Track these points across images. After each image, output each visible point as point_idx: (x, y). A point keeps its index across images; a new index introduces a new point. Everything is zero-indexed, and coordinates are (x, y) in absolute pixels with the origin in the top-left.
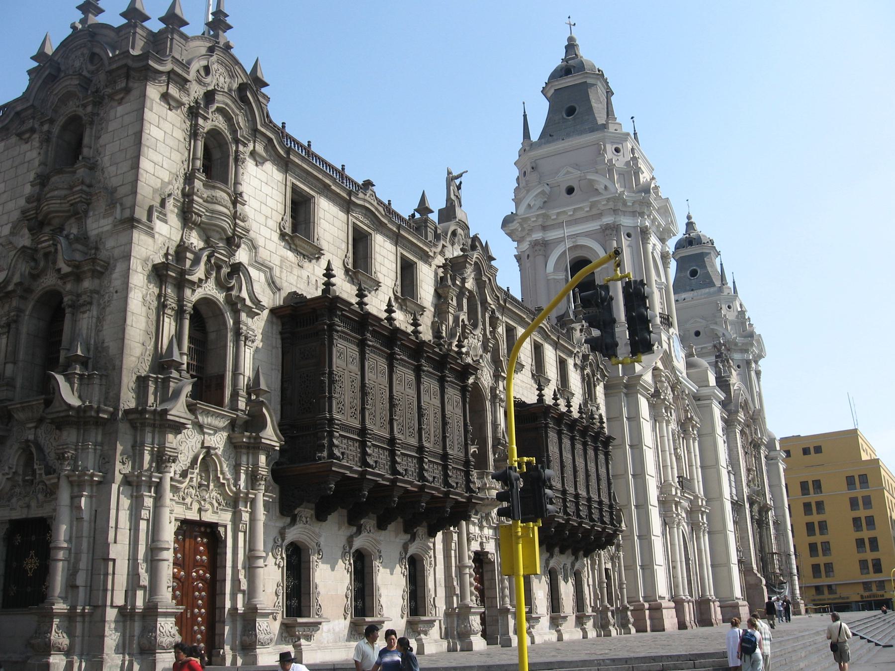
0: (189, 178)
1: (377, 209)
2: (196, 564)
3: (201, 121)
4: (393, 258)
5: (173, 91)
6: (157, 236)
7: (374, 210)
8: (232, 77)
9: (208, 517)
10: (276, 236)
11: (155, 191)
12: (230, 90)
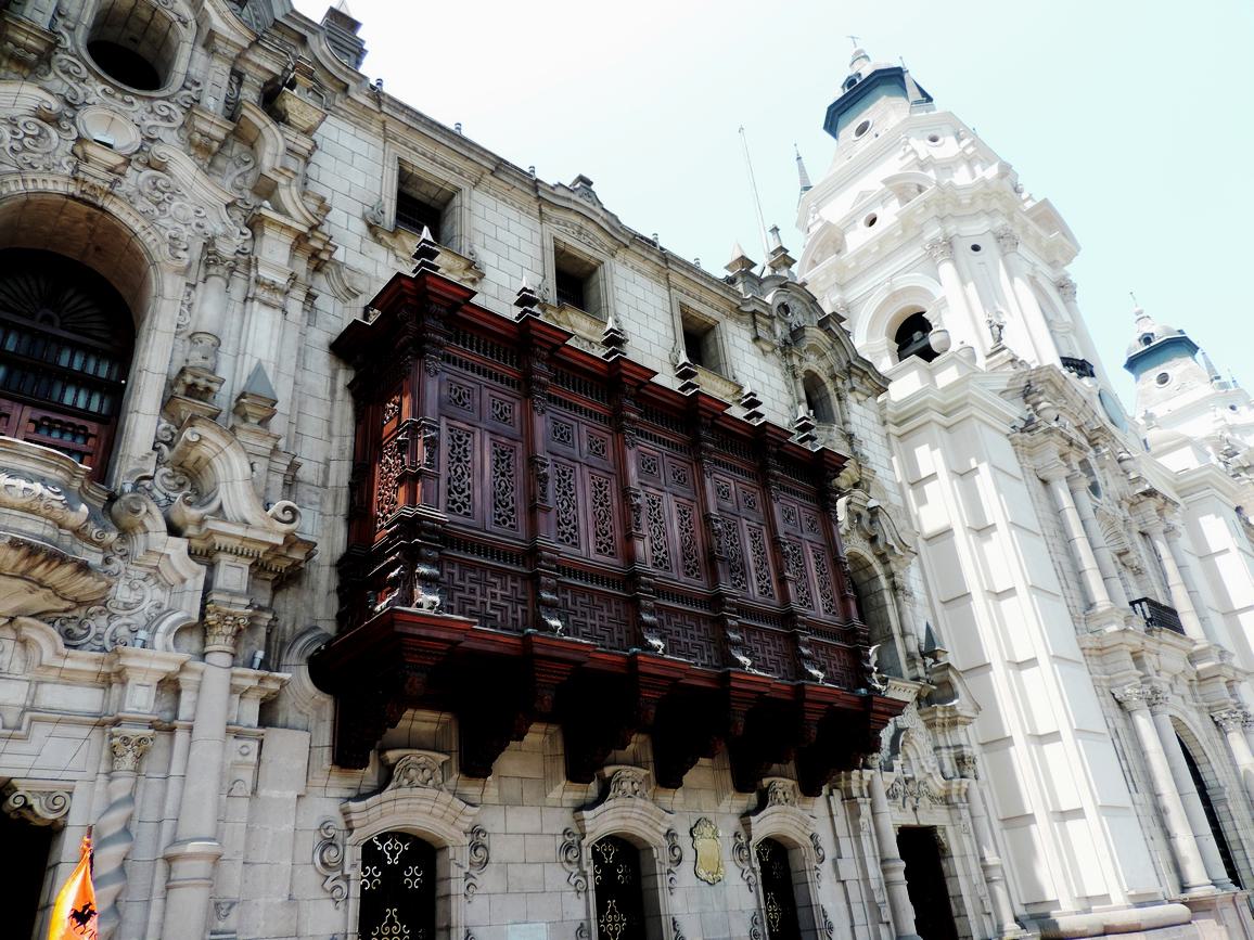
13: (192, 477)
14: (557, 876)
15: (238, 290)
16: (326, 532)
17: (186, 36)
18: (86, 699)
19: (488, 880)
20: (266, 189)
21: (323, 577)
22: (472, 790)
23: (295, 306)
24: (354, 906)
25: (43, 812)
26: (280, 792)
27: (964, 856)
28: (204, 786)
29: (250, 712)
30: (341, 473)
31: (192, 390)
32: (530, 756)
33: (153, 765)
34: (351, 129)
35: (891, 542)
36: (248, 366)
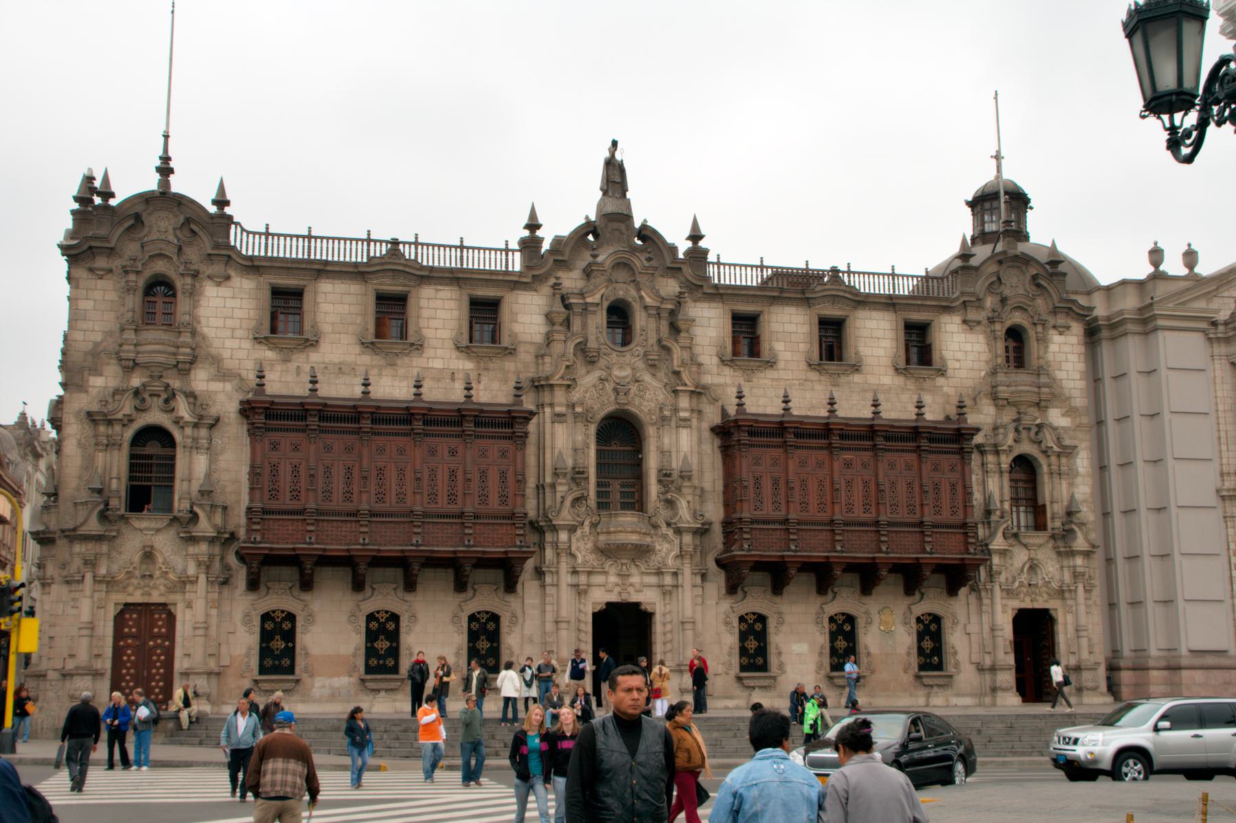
0: (122, 330)
1: (405, 266)
2: (154, 637)
3: (132, 277)
4: (452, 304)
5: (101, 262)
6: (90, 389)
7: (401, 268)
8: (176, 216)
9: (156, 598)
10: (247, 344)
11: (86, 354)
12: (175, 229)
13: (670, 503)
14: (812, 628)
15: (673, 424)
16: (714, 512)
17: (636, 307)
18: (653, 580)
19: (784, 628)
20: (677, 373)
21: (717, 529)
22: (777, 599)
23: (694, 422)
24: (737, 636)
25: (650, 609)
26: (711, 602)
27: (1065, 624)
28: (688, 603)
29: (699, 579)
30: (720, 486)
31: (666, 475)
32: (800, 586)
33: (674, 594)
34: (707, 305)
35: (1051, 444)
36: (682, 455)
